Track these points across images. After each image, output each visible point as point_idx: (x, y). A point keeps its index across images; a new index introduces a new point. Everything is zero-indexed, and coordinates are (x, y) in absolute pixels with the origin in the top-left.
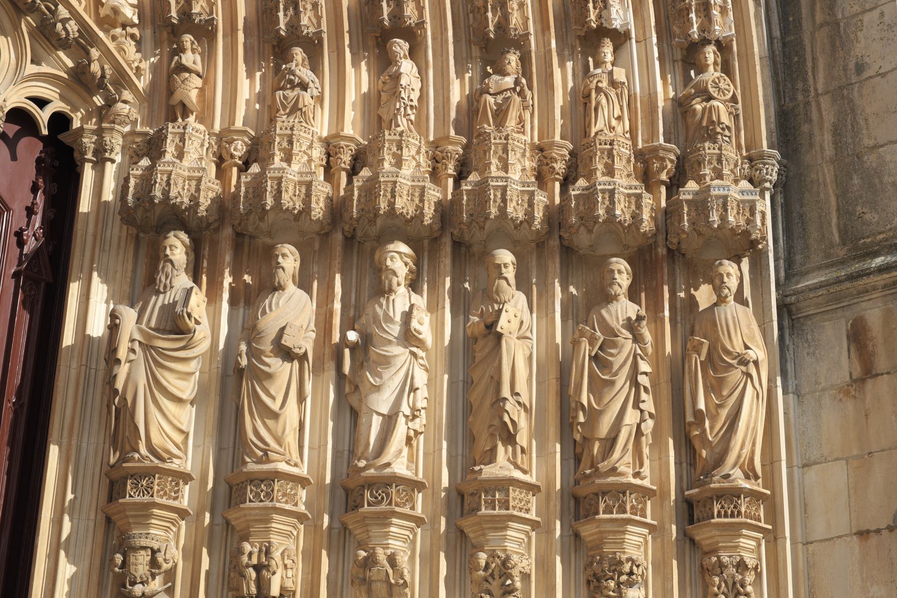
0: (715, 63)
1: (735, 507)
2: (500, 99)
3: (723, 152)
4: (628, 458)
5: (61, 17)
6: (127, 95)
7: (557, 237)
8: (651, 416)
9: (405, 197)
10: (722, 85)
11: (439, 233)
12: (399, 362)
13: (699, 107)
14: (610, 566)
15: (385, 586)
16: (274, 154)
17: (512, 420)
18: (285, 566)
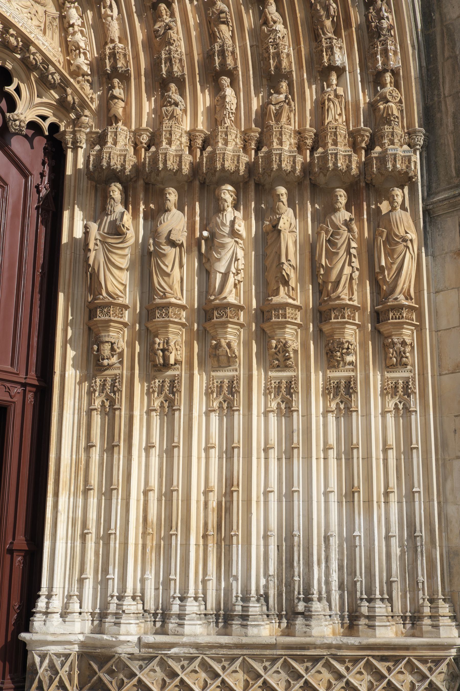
0: (391, 82)
1: (400, 314)
4: (346, 291)
5: (51, 72)
6: (87, 112)
7: (308, 179)
8: (357, 269)
9: (230, 161)
10: (394, 94)
12: (229, 246)
13: (382, 107)
15: (226, 358)
16: (162, 141)
17: (287, 274)
18: (177, 349)
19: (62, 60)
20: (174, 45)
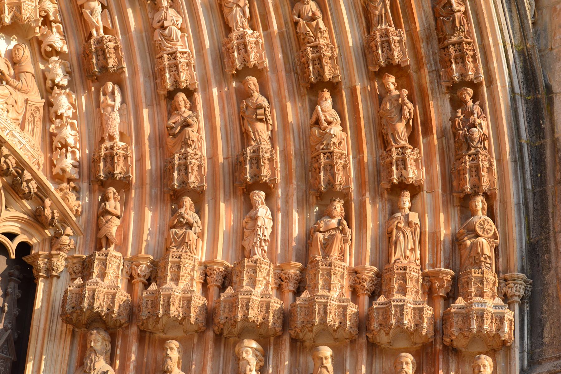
0: (483, 209)
2: (327, 235)
3: (485, 276)
7: (364, 336)
9: (256, 310)
10: (487, 227)
11: (281, 333)
13: (469, 242)
19: (42, 160)
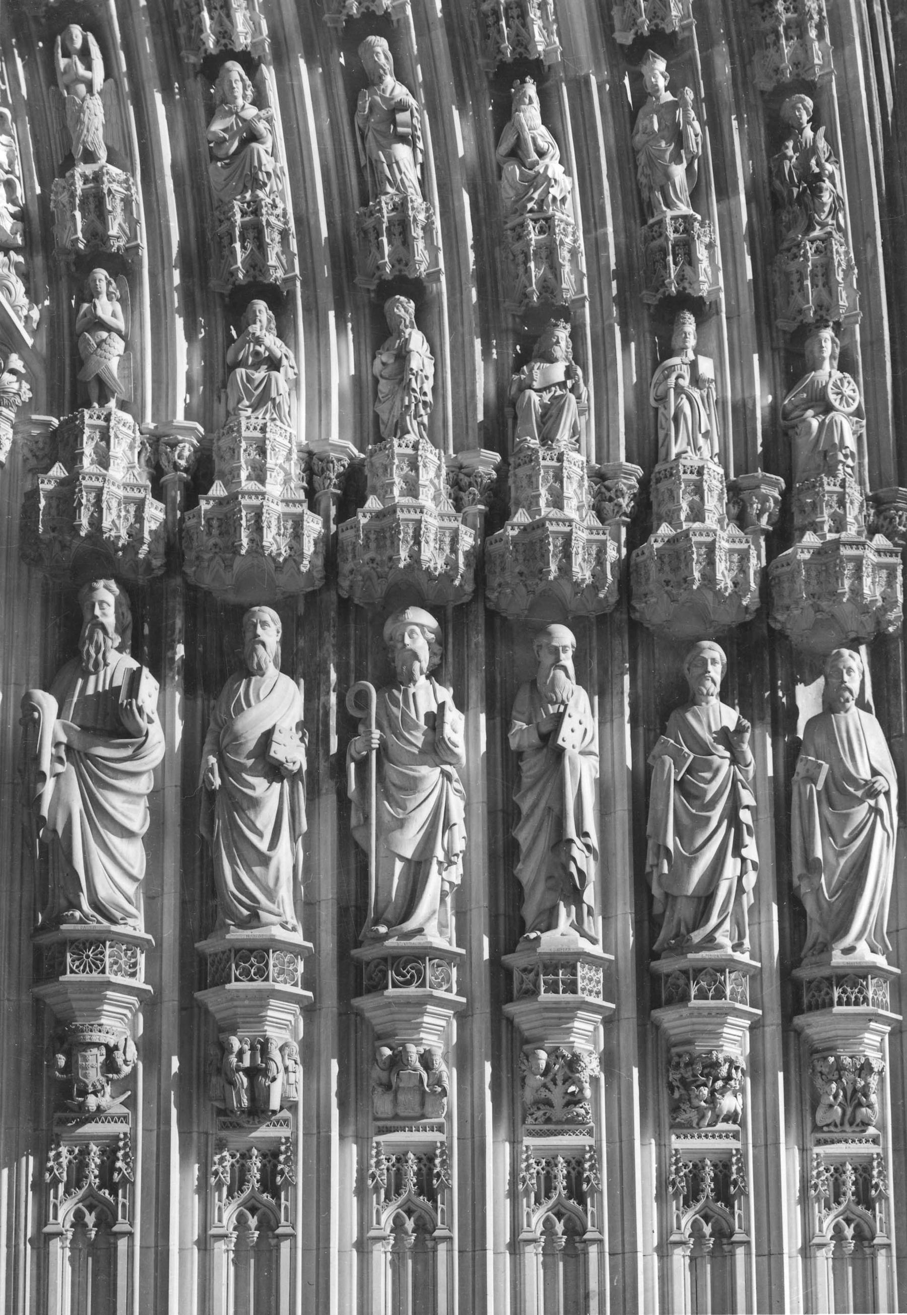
1: (860, 992)
2: (547, 397)
3: (848, 490)
8: (755, 866)
12: (427, 786)
13: (815, 424)
14: (704, 1067)
16: (239, 468)
17: (580, 872)
18: (286, 1069)
20: (268, 189)
